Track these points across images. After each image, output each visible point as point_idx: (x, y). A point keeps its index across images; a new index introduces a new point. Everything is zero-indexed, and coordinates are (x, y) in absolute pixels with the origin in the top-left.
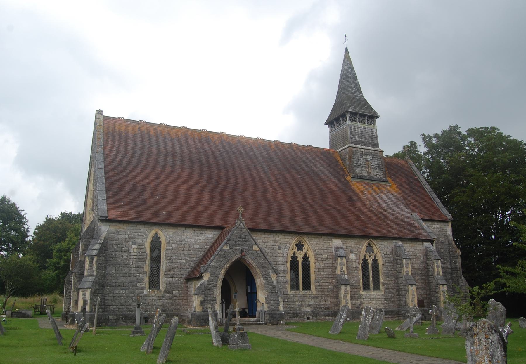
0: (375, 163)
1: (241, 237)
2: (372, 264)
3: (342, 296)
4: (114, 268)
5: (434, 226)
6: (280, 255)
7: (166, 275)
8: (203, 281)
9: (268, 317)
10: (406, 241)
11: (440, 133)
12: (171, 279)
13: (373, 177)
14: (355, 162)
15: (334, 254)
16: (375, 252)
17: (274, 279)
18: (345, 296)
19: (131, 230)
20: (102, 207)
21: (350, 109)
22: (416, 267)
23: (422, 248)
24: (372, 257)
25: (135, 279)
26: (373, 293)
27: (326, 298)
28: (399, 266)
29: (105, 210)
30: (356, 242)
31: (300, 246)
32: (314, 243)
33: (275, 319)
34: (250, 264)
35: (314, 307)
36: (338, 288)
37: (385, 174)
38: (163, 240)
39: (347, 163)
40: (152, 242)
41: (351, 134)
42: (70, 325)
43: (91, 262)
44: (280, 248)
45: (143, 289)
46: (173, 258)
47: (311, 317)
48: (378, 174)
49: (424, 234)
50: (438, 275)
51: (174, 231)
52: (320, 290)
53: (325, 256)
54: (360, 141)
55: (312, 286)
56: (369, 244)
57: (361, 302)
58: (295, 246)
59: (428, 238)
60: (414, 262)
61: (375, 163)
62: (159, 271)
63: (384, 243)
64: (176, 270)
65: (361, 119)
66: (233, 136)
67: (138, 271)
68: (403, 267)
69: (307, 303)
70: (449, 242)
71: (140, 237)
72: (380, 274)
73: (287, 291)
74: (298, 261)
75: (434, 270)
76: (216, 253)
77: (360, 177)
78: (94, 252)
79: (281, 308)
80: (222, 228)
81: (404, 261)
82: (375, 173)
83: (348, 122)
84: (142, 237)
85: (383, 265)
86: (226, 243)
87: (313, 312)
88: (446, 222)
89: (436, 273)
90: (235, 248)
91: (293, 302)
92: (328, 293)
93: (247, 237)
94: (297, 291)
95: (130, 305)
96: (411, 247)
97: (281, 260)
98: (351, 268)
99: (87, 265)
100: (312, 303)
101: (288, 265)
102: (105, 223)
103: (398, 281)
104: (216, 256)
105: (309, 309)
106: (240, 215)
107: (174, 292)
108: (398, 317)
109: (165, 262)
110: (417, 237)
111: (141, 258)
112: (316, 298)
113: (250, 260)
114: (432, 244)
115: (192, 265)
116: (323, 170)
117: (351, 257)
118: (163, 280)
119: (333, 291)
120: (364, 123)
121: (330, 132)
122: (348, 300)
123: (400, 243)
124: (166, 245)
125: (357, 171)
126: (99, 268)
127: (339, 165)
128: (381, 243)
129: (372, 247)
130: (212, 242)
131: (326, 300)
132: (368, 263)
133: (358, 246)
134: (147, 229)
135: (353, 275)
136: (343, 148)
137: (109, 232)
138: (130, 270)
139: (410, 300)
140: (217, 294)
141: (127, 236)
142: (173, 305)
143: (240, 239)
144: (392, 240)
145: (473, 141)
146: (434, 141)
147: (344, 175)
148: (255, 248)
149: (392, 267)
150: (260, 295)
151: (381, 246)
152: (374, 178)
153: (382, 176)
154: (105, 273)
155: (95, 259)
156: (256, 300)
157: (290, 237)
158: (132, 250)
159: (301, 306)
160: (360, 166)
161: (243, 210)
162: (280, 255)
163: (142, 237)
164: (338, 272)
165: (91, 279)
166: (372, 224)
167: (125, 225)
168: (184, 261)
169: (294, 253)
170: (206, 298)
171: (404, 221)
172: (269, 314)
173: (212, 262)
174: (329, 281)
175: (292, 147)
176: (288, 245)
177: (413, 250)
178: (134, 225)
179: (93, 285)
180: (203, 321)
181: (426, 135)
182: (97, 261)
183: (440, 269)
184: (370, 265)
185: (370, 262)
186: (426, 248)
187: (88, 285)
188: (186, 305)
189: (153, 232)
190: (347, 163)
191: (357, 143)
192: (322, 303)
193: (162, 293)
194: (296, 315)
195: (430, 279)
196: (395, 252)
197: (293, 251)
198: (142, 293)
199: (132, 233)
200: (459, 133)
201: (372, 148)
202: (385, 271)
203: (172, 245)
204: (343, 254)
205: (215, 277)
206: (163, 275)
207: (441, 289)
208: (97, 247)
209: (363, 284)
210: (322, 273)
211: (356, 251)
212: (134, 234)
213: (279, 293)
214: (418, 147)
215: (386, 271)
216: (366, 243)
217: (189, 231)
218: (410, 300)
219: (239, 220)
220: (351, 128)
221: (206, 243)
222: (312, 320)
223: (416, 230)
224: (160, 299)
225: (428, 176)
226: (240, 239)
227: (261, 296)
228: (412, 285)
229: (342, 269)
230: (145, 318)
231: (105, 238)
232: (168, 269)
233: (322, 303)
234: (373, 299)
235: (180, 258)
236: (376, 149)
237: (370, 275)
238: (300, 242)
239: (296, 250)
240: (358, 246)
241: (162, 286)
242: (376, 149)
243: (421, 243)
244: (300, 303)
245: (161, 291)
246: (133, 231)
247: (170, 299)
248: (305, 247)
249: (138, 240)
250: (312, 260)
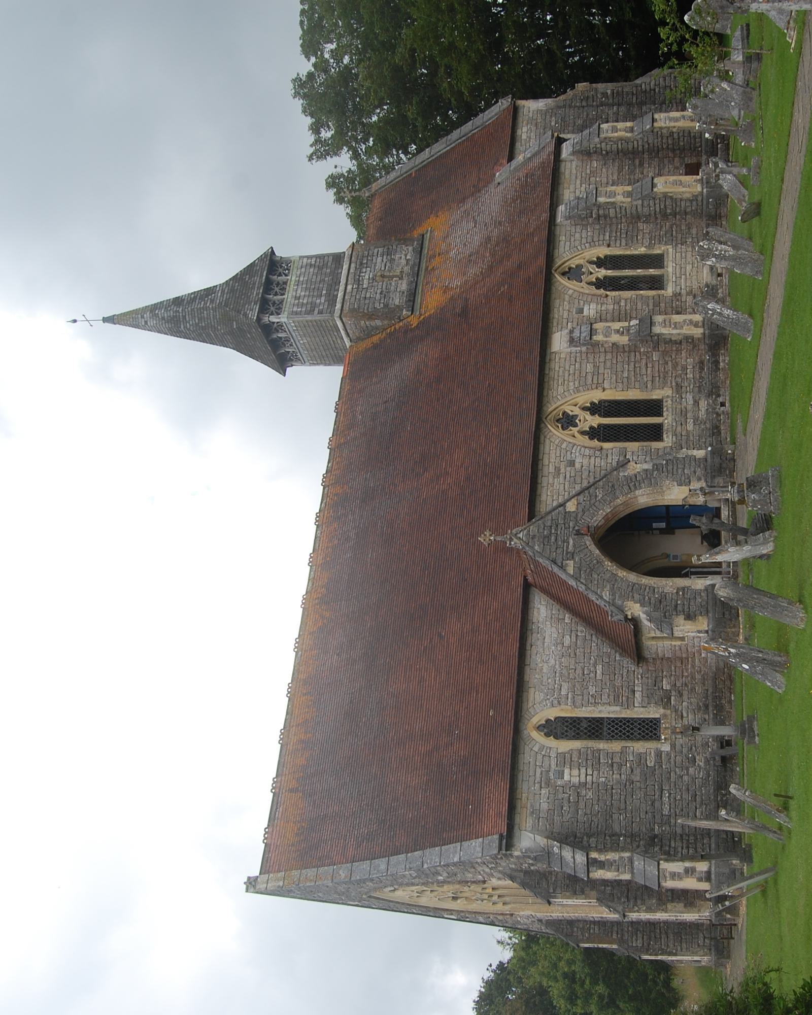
0: (379, 262)
1: (548, 537)
2: (606, 269)
3: (675, 332)
4: (615, 816)
5: (524, 137)
6: (586, 462)
7: (630, 704)
8: (643, 617)
9: (720, 480)
11: (309, 120)
12: (638, 695)
13: (412, 268)
14: (377, 305)
15: (584, 349)
16: (581, 262)
17: (639, 468)
18: (676, 325)
19: (531, 783)
20: (479, 849)
21: (253, 315)
22: (615, 177)
23: (574, 163)
24: (592, 268)
25: (637, 771)
26: (670, 269)
27: (679, 368)
28: (612, 211)
29: (486, 842)
30: (558, 301)
31: (568, 421)
32: (561, 389)
33: (724, 465)
34: (606, 518)
35: (700, 391)
36: (657, 342)
37: (406, 241)
38: (553, 713)
39: (378, 323)
40: (556, 738)
41: (311, 312)
42: (738, 916)
43: (601, 865)
44: (572, 463)
45: (659, 754)
46: (592, 690)
47: (721, 400)
48: (404, 256)
49: (544, 156)
50: (631, 130)
51: (532, 691)
52: (662, 379)
53: (590, 368)
54: (328, 294)
55: (654, 397)
56: (564, 274)
57: (688, 294)
58: (565, 432)
59: (551, 148)
60: (604, 180)
61: (379, 262)
62: (621, 720)
63: (562, 243)
64: (618, 683)
65: (277, 289)
66: (312, 580)
67: (620, 766)
68: (614, 203)
69: (689, 407)
70: (560, 107)
71: (546, 763)
72: (628, 252)
73: (665, 448)
74: (599, 425)
75: (621, 139)
76: (582, 588)
77: (412, 296)
78: (580, 858)
79: (700, 453)
80: (527, 587)
81: (601, 200)
82: (403, 262)
83: (283, 318)
84: (546, 759)
85: (609, 246)
86: (562, 567)
87: (710, 395)
88: (515, 110)
89: (629, 135)
90: (571, 548)
91: (688, 436)
92: (670, 363)
93: (549, 523)
94: (665, 428)
95: (694, 779)
96: (572, 187)
97: (598, 460)
98: (616, 314)
99: (609, 875)
100: (690, 398)
101: (607, 445)
102: (515, 840)
103: (645, 216)
104: (587, 588)
105: (703, 404)
106: (499, 539)
107: (666, 686)
108: (720, 217)
109: (600, 708)
110: (550, 171)
111: (593, 760)
112: (679, 388)
113: (598, 518)
114: (565, 140)
115: (607, 649)
116: (400, 372)
117: (592, 313)
118: (639, 712)
119: (665, 353)
120: (285, 283)
121: (303, 363)
122: (685, 321)
123: (561, 208)
124: (563, 707)
125: (397, 302)
126: (616, 847)
127: (382, 341)
128: (561, 249)
129: (570, 268)
130: (556, 606)
131: (685, 368)
132: (605, 277)
133: (567, 297)
134: (527, 749)
135: (631, 310)
136: (343, 332)
137: (535, 830)
138: (619, 782)
139: (684, 189)
140: (669, 585)
141: (543, 791)
142: (693, 689)
143: (553, 538)
144: (555, 225)
145: (333, 46)
146: (326, 134)
147: (407, 330)
148: (571, 507)
149: (614, 227)
150: (673, 497)
151: (567, 248)
152: (414, 264)
153: (410, 248)
154: (625, 836)
155: (594, 855)
156: (683, 506)
157: (547, 441)
158: (575, 780)
159: (696, 420)
160: (385, 294)
161: (487, 533)
162: (586, 462)
163: (546, 759)
164: (624, 340)
165: (638, 863)
166: (519, 267)
167: (519, 796)
168: (599, 668)
169: (583, 433)
170: (680, 608)
171: (514, 201)
172: (713, 477)
173: (601, 597)
174: (644, 362)
175: (337, 447)
176: (564, 446)
177: (578, 182)
178: (520, 777)
179: (652, 857)
180: (727, 613)
181: (312, 150)
182: (600, 851)
183: (620, 125)
184: (610, 273)
185: (603, 273)
186: (574, 153)
187: (652, 869)
188: (693, 661)
189: (535, 734)
190: (378, 323)
191: (332, 301)
192: (690, 376)
193: (669, 712)
194: (716, 430)
195: (640, 148)
196: (583, 219)
197: (577, 434)
198: (668, 754)
199: (538, 779)
200: (310, 76)
201: (345, 267)
202: (623, 243)
203: (563, 692)
204: (585, 329)
205: (633, 591)
206: (628, 712)
207: (663, 125)
208: (567, 853)
209: (650, 289)
210: (626, 375)
211: (577, 303)
212: (538, 774)
213: (668, 457)
214: (339, 170)
215: (623, 241)
216: (561, 281)
217: (533, 657)
218: (684, 189)
219: (511, 540)
220: (296, 313)
221: (559, 620)
222: (725, 397)
223: (533, 175)
224: (682, 717)
225: (406, 153)
226: (553, 538)
227: (675, 494)
228: (653, 185)
229: (618, 331)
230: (722, 747)
231: (547, 838)
232: (616, 700)
233: (690, 376)
234: (684, 268)
235: (592, 675)
236: (346, 260)
237: (630, 275)
238: (558, 421)
239: (575, 430)
240: (567, 297)
241: (654, 712)
242: (346, 260)
243: (563, 165)
244: (690, 421)
245: (665, 716)
246: (532, 779)
247: (681, 695)
248: (568, 409)
249: (553, 766)
250: (597, 396)
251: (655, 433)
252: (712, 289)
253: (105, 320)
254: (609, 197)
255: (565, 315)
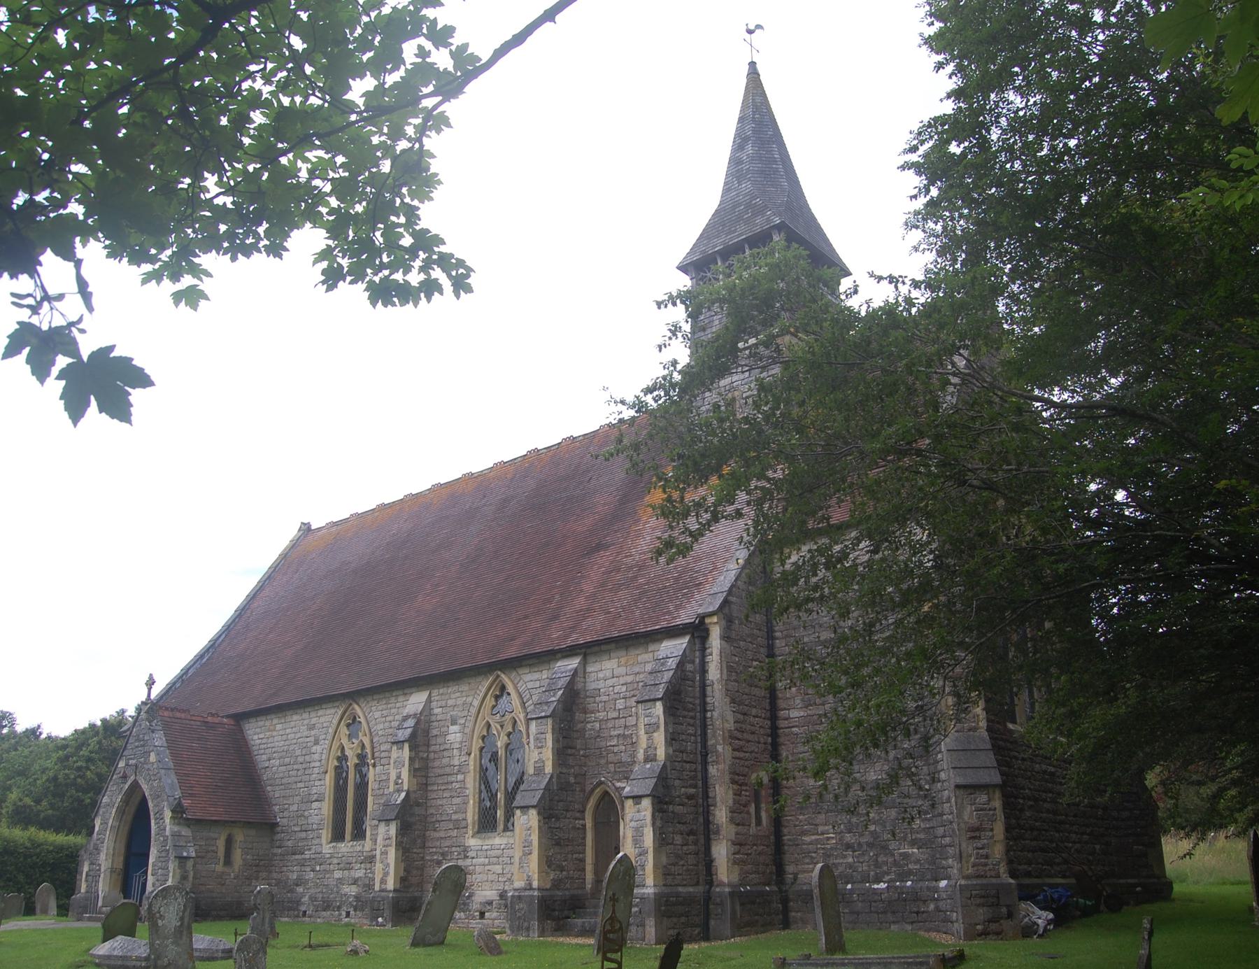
10: (609, 651)
32: (377, 714)
47: (352, 912)
63: (536, 676)
69: (352, 872)
87: (357, 898)
94: (339, 845)
96: (622, 670)
98: (448, 770)
128: (527, 677)
133: (470, 699)
151: (530, 685)
177: (629, 679)
183: (660, 738)
229: (399, 777)
251: (338, 836)
252: (464, 904)
253: (752, 65)
254: (537, 739)
255: (450, 702)
